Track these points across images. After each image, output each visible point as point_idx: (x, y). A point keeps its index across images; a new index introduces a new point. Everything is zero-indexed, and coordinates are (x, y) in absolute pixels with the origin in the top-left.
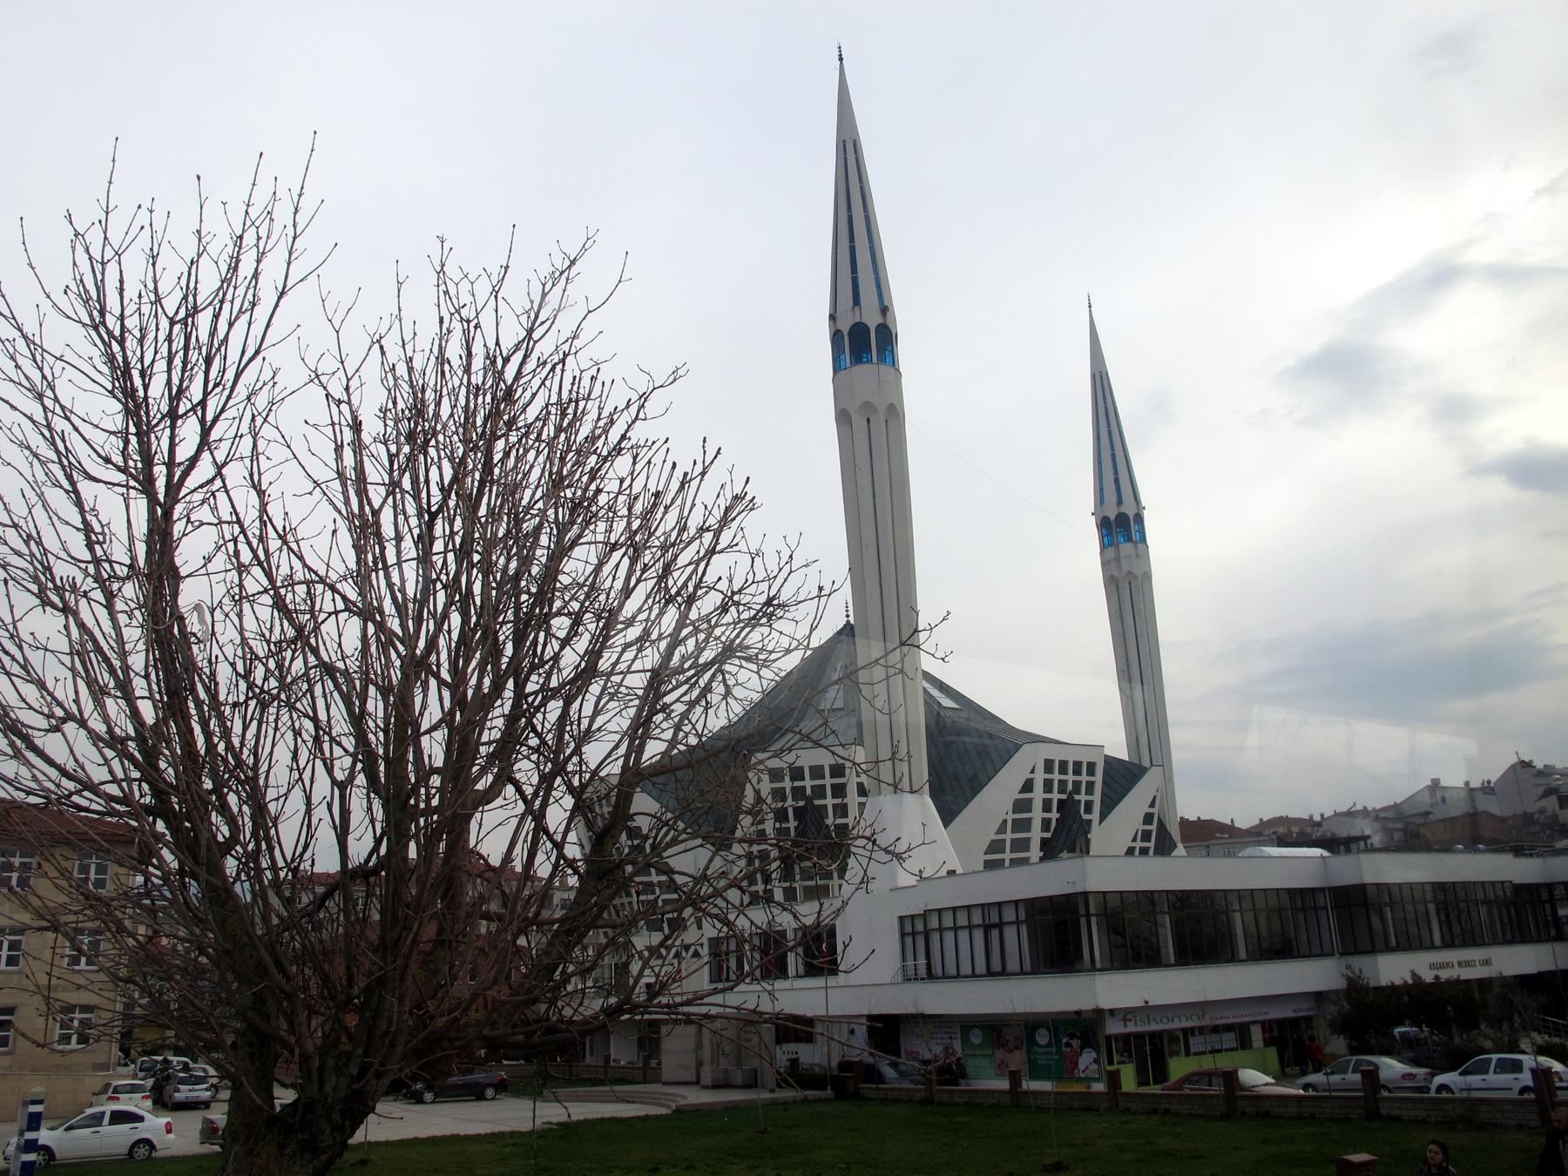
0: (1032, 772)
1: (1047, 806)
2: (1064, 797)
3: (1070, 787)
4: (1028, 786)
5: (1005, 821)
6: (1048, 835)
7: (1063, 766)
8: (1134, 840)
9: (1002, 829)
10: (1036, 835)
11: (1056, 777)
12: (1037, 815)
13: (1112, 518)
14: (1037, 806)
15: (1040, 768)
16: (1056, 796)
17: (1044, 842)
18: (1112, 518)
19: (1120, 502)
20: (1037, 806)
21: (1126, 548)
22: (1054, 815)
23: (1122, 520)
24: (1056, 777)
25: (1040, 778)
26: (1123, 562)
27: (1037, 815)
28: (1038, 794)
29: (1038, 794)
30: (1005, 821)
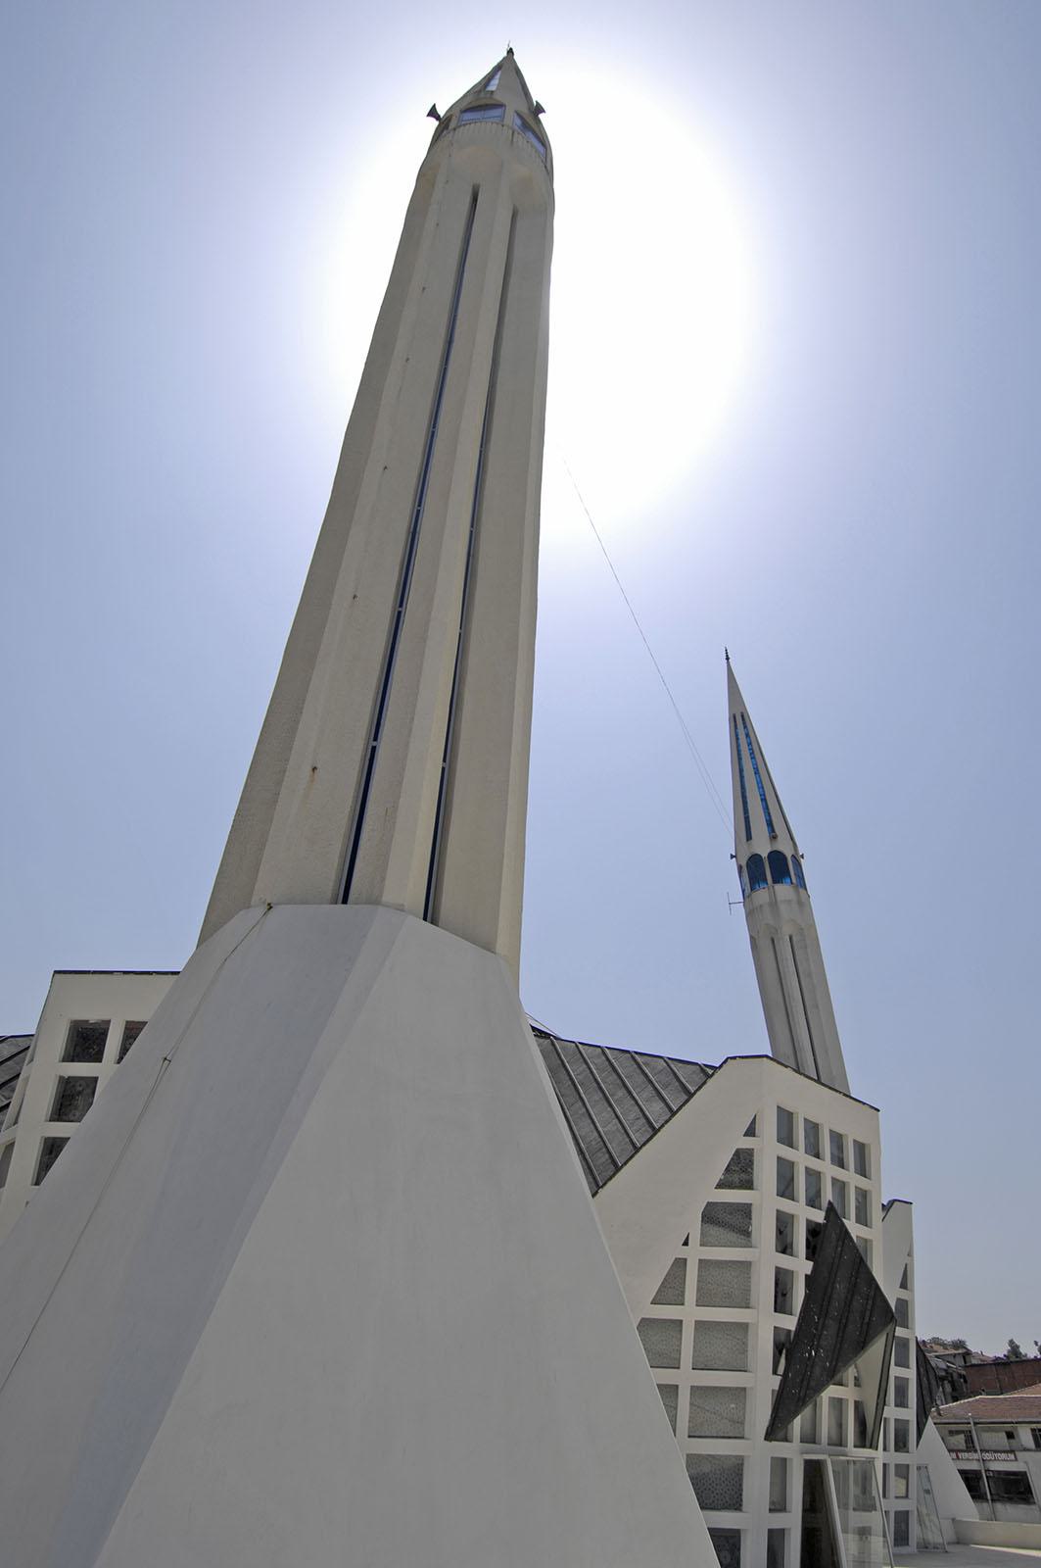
0: (751, 1132)
2: (819, 1217)
3: (828, 1195)
4: (740, 1172)
5: (680, 1264)
9: (670, 1290)
10: (766, 1323)
11: (801, 1159)
13: (764, 855)
14: (764, 1229)
15: (769, 1127)
16: (805, 1214)
17: (784, 1345)
18: (764, 855)
19: (774, 837)
20: (764, 1229)
21: (783, 890)
22: (801, 1266)
23: (777, 858)
24: (801, 1159)
26: (783, 908)
29: (764, 1200)
30: (680, 1264)
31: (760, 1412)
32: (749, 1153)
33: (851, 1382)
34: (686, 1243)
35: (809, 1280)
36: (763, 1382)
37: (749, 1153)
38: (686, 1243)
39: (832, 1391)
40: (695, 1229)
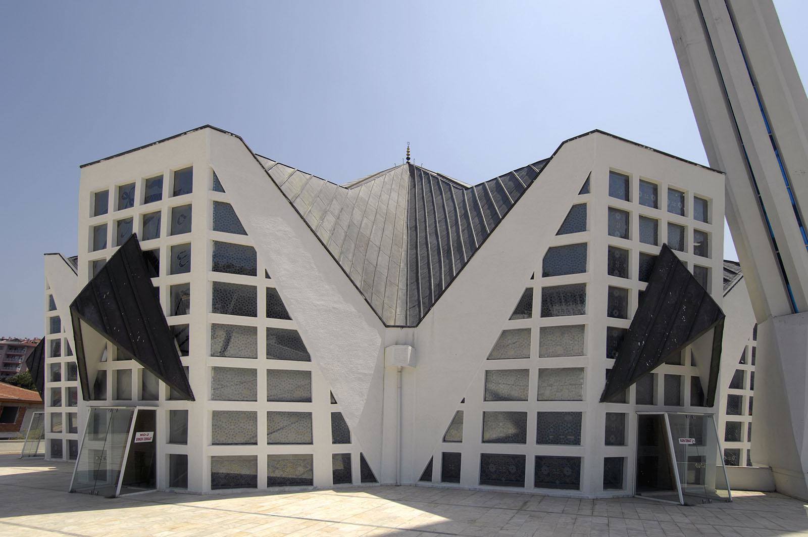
0: (585, 189)
1: (617, 263)
2: (655, 251)
6: (624, 324)
7: (651, 192)
8: (743, 361)
12: (596, 280)
14: (597, 260)
16: (636, 247)
20: (597, 260)
22: (634, 285)
24: (635, 208)
25: (599, 204)
27: (596, 280)
28: (597, 239)
29: (597, 239)
31: (595, 381)
32: (584, 206)
33: (688, 361)
34: (532, 278)
35: (641, 293)
36: (595, 362)
37: (584, 206)
38: (532, 278)
39: (663, 370)
40: (539, 270)
